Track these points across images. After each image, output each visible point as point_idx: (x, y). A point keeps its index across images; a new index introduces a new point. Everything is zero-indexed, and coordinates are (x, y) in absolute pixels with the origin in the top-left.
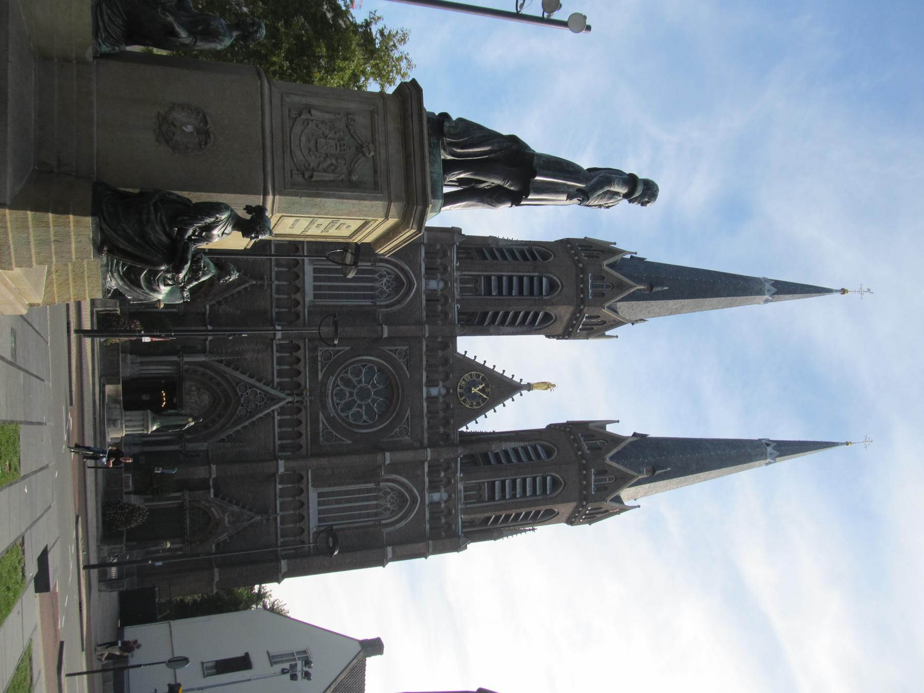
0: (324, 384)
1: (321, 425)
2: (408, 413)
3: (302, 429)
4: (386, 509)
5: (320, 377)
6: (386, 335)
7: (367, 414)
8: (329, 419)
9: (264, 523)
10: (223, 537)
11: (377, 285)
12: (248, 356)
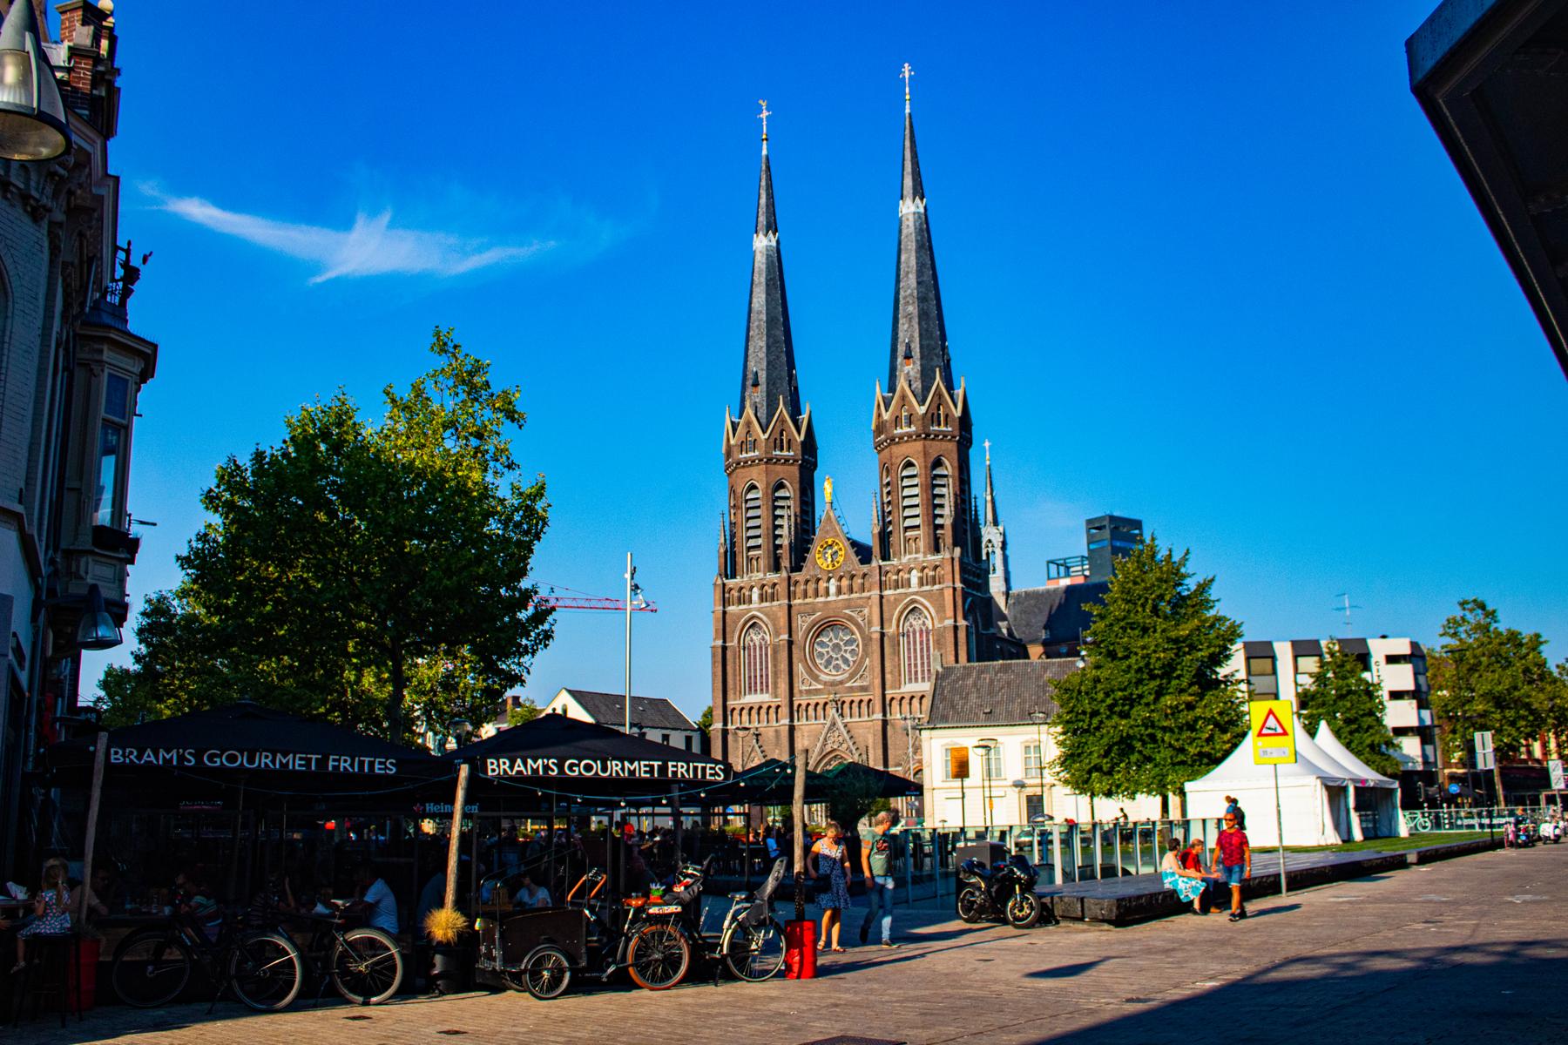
0: (825, 683)
8: (851, 676)
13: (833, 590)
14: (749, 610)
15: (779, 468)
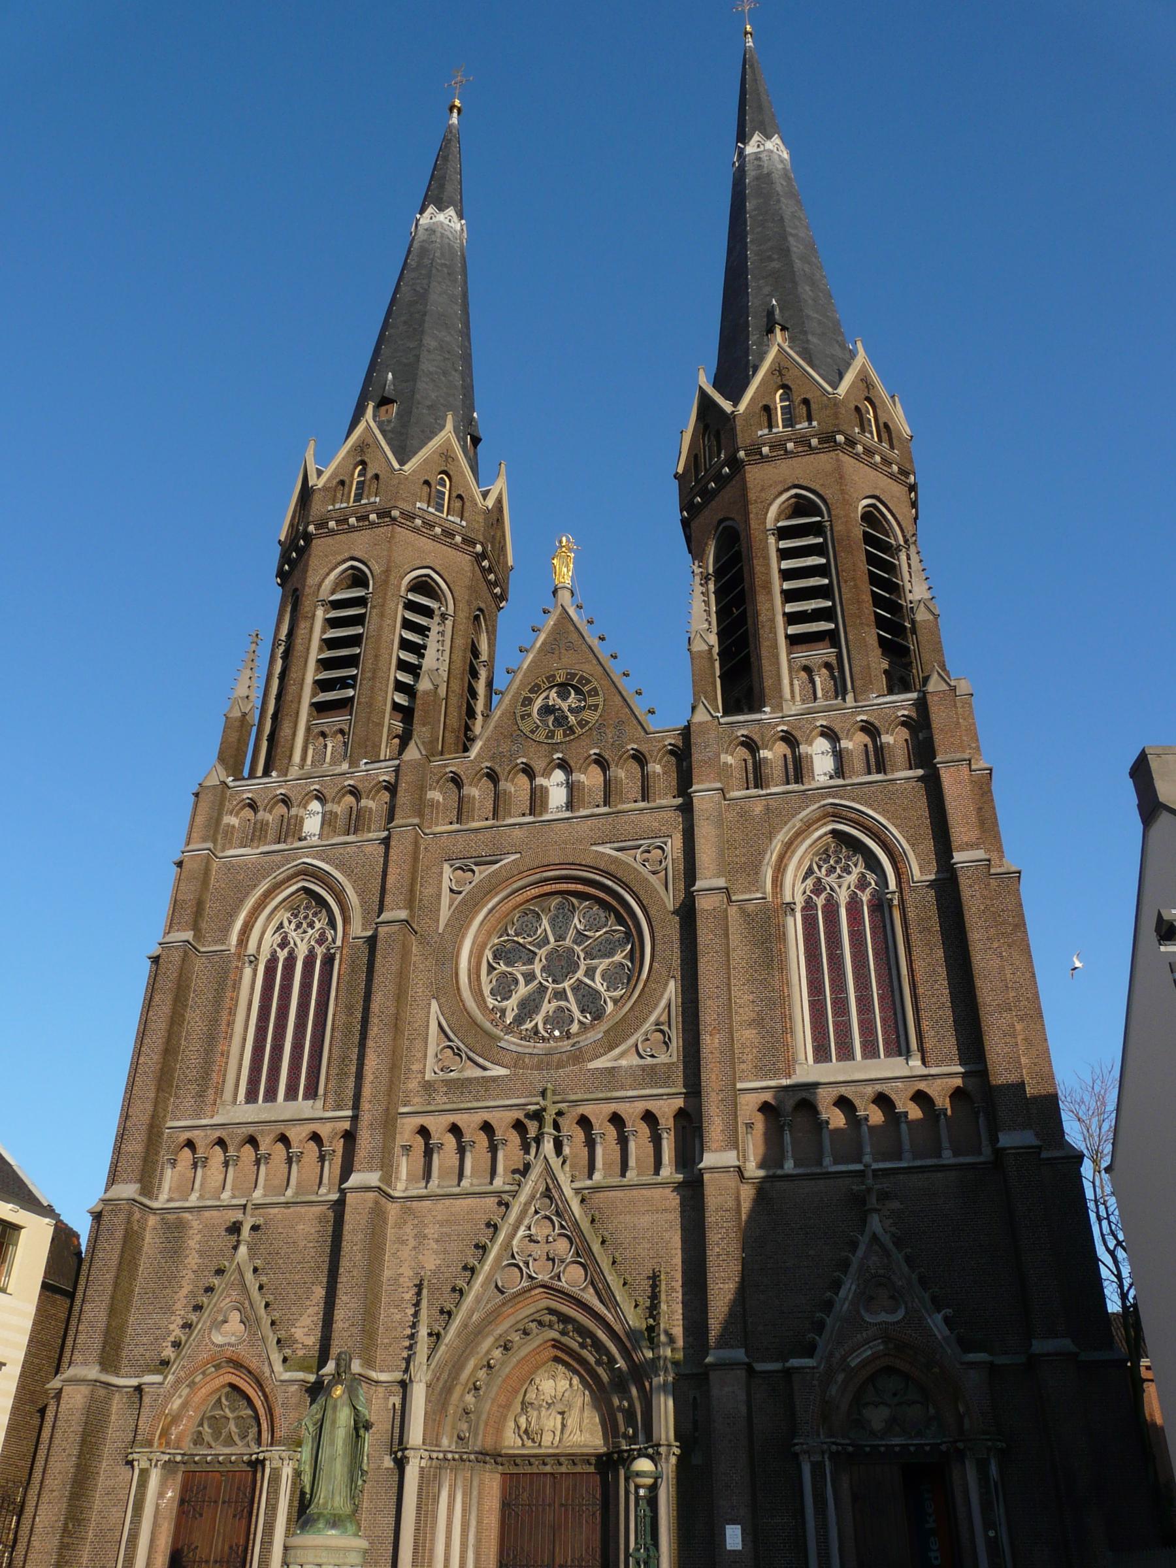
0: (517, 1061)
1: (624, 1062)
2: (606, 850)
4: (862, 884)
5: (502, 1071)
6: (403, 914)
7: (611, 954)
9: (895, 1205)
10: (936, 1323)
11: (302, 952)
12: (431, 1262)
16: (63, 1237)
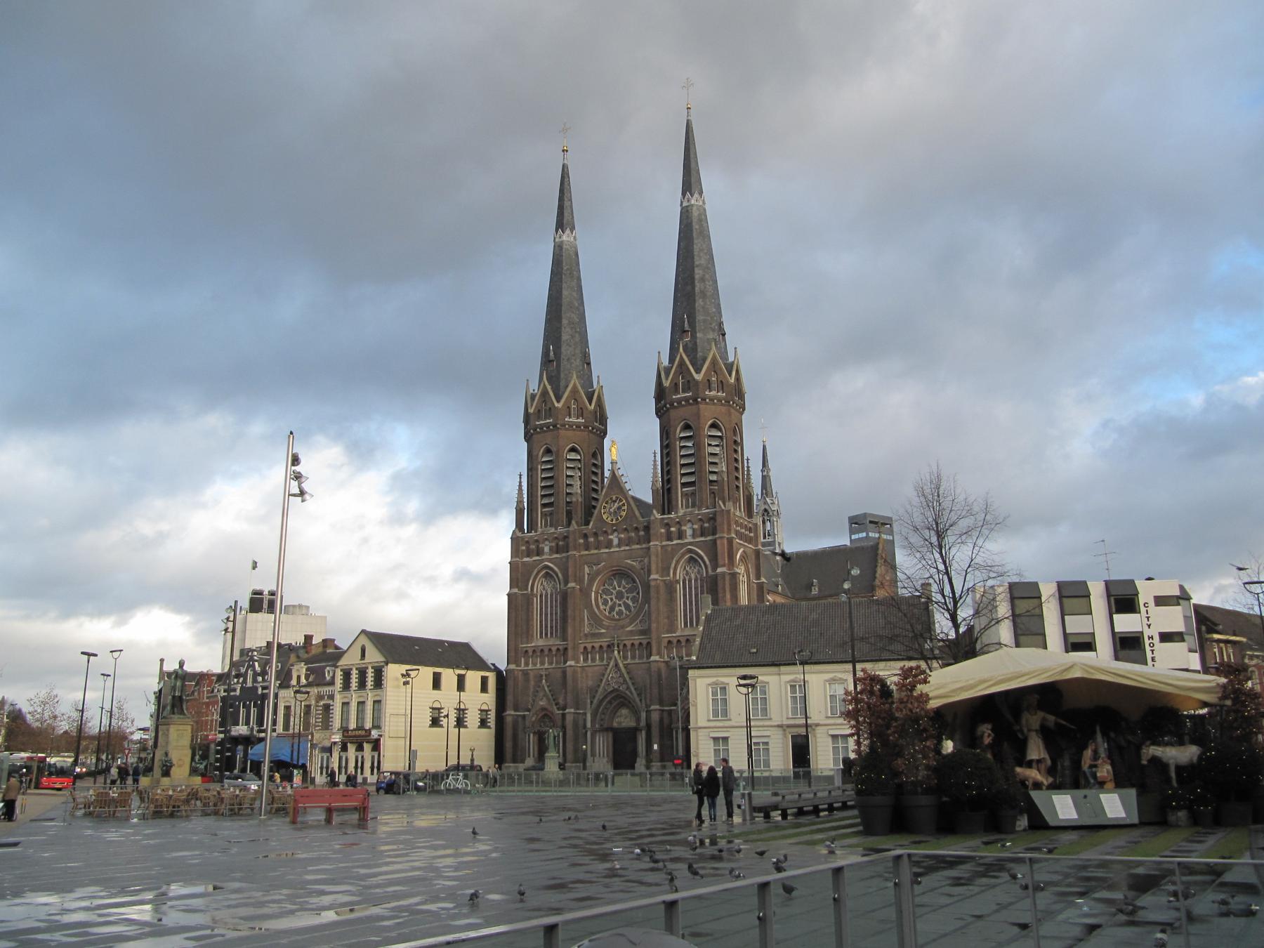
3: (637, 643)
12: (590, 683)
13: (616, 541)
14: (542, 561)
15: (570, 433)
16: (499, 673)
